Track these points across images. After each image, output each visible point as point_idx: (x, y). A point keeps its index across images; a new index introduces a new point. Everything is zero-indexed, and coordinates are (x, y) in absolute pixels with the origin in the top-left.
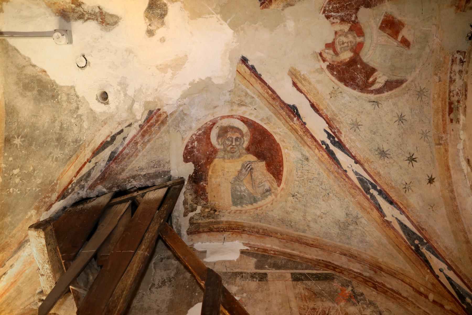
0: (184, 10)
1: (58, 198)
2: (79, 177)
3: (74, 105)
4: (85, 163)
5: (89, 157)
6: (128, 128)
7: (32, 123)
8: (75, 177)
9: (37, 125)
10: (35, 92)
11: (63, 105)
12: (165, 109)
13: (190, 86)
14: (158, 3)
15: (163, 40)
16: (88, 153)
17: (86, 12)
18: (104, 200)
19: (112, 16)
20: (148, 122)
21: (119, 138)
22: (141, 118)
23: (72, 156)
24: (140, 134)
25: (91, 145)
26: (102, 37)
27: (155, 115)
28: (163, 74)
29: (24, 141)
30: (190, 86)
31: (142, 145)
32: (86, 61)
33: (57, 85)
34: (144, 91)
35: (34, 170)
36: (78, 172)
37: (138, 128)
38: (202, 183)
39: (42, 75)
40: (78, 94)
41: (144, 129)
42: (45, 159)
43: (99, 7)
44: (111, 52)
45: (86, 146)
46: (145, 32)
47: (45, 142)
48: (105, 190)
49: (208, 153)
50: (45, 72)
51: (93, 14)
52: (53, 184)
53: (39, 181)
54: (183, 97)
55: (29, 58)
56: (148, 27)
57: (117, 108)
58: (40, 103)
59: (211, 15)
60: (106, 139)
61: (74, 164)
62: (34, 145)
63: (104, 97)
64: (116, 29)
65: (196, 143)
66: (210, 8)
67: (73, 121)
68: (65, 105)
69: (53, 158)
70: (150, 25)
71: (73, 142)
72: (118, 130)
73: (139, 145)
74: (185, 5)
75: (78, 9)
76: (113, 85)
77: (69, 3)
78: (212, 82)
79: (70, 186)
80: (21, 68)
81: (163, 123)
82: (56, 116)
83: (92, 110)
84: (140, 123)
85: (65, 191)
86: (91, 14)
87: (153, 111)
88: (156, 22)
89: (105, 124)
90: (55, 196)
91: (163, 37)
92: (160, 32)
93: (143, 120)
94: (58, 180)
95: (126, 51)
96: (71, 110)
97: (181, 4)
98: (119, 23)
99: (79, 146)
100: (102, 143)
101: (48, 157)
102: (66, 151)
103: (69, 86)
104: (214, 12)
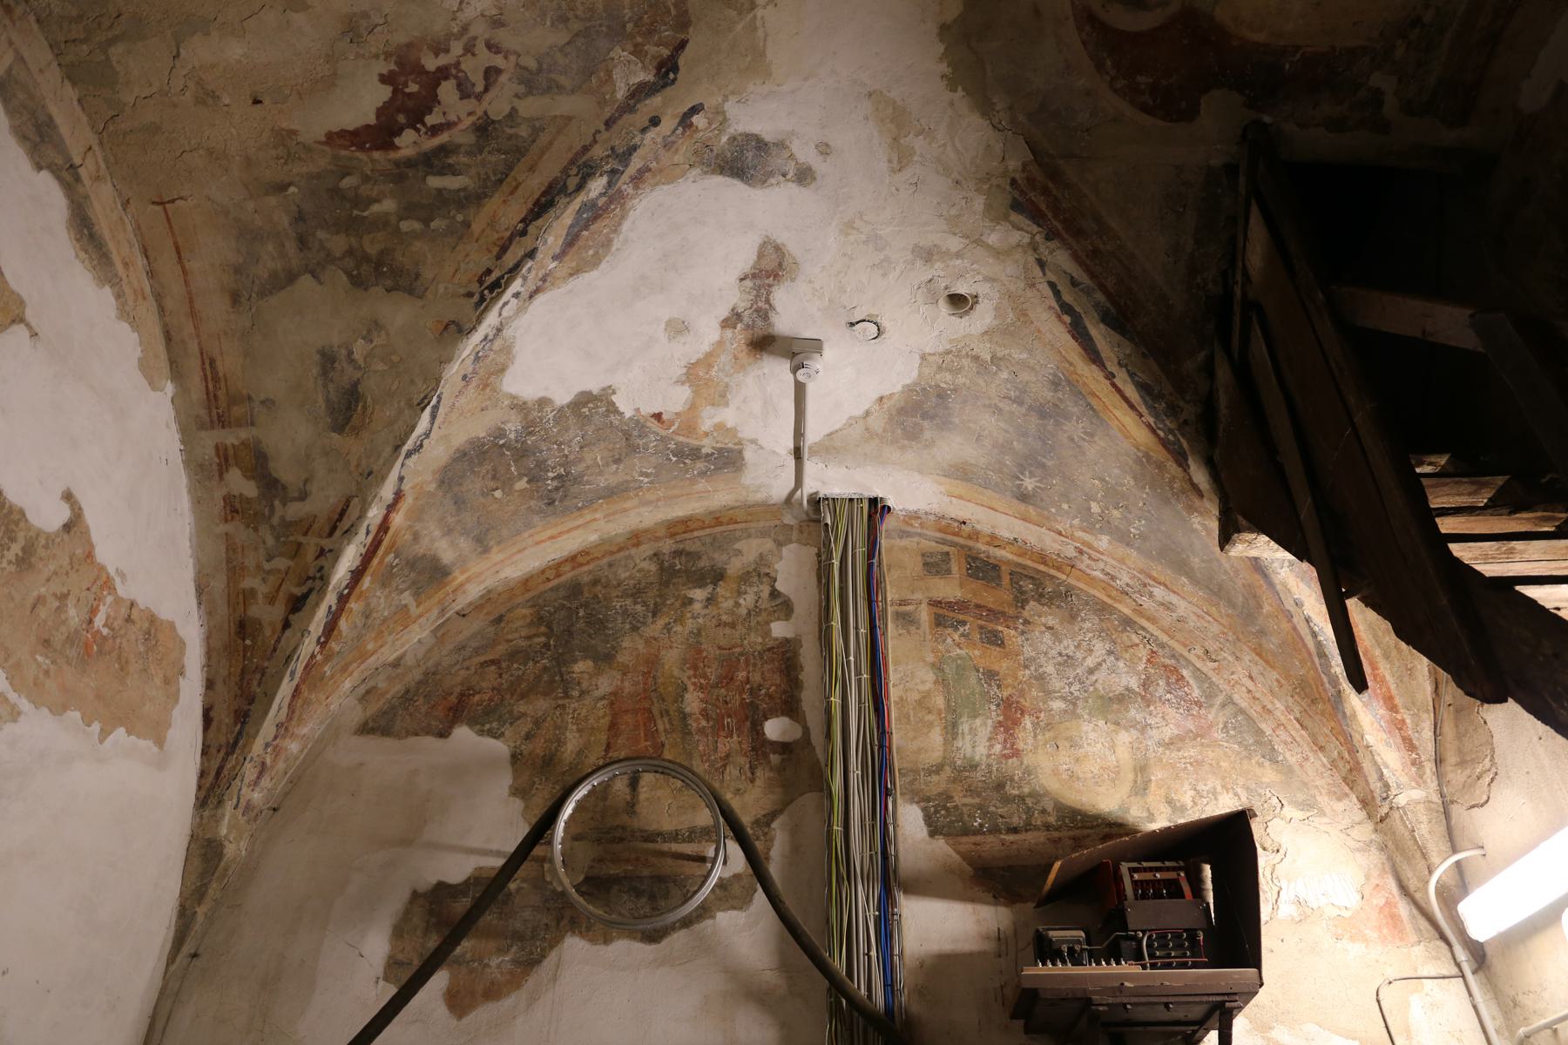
0: (745, 95)
1: (1180, 465)
2: (1143, 409)
3: (966, 362)
4: (1114, 385)
5: (1102, 374)
6: (1047, 271)
7: (993, 447)
8: (1141, 416)
9: (1001, 440)
10: (926, 424)
11: (964, 384)
12: (1013, 164)
13: (960, 88)
14: (729, 155)
15: (824, 149)
16: (1090, 374)
17: (752, 305)
18: (1223, 373)
19: (761, 255)
20: (1043, 216)
21: (1067, 298)
22: (1028, 233)
23: (1089, 404)
24: (1070, 240)
25: (1071, 360)
26: (810, 282)
27: (1026, 194)
28: (916, 158)
29: (1030, 472)
30: (960, 88)
31: (1105, 238)
32: (864, 321)
33: (915, 384)
34: (953, 212)
35: (1102, 480)
36: (1132, 406)
37: (1053, 244)
38: (1287, 66)
39: (887, 404)
40: (941, 349)
41: (1060, 227)
42: (1084, 454)
43: (742, 280)
44: (849, 267)
45: (1072, 368)
46: (803, 189)
47: (1043, 441)
48: (1203, 354)
49: (1185, 42)
50: (881, 399)
51: (758, 292)
52: (1144, 460)
53: (1129, 481)
54: (985, 107)
55: (850, 418)
56: (788, 180)
57: (987, 279)
58: (951, 423)
59: (758, 23)
60: (1065, 323)
61: (1110, 407)
62: (1044, 460)
63: (957, 301)
64: (793, 247)
65: (1141, 79)
66: (739, 27)
67: (1004, 375)
68: (964, 380)
69: (1084, 439)
70: (784, 175)
71: (1056, 391)
72: (1048, 292)
73: (1101, 246)
74: (733, 93)
75: (746, 320)
76: (930, 277)
77: (733, 332)
78: (955, 21)
79: (1161, 434)
80: (870, 434)
81: (1054, 174)
82: (987, 402)
83: (986, 333)
84: (1038, 238)
85: (1171, 447)
86: (756, 296)
87: (1014, 199)
88: (777, 161)
89: (1026, 315)
90: (1172, 466)
91: (817, 146)
92: (805, 153)
93: (1035, 229)
94: (1138, 449)
95: (847, 234)
96: (978, 373)
97: (730, 102)
98: (779, 241)
99: (1069, 382)
100: (1073, 337)
101: (1079, 447)
102: (1075, 410)
103: (921, 364)
104: (751, 15)
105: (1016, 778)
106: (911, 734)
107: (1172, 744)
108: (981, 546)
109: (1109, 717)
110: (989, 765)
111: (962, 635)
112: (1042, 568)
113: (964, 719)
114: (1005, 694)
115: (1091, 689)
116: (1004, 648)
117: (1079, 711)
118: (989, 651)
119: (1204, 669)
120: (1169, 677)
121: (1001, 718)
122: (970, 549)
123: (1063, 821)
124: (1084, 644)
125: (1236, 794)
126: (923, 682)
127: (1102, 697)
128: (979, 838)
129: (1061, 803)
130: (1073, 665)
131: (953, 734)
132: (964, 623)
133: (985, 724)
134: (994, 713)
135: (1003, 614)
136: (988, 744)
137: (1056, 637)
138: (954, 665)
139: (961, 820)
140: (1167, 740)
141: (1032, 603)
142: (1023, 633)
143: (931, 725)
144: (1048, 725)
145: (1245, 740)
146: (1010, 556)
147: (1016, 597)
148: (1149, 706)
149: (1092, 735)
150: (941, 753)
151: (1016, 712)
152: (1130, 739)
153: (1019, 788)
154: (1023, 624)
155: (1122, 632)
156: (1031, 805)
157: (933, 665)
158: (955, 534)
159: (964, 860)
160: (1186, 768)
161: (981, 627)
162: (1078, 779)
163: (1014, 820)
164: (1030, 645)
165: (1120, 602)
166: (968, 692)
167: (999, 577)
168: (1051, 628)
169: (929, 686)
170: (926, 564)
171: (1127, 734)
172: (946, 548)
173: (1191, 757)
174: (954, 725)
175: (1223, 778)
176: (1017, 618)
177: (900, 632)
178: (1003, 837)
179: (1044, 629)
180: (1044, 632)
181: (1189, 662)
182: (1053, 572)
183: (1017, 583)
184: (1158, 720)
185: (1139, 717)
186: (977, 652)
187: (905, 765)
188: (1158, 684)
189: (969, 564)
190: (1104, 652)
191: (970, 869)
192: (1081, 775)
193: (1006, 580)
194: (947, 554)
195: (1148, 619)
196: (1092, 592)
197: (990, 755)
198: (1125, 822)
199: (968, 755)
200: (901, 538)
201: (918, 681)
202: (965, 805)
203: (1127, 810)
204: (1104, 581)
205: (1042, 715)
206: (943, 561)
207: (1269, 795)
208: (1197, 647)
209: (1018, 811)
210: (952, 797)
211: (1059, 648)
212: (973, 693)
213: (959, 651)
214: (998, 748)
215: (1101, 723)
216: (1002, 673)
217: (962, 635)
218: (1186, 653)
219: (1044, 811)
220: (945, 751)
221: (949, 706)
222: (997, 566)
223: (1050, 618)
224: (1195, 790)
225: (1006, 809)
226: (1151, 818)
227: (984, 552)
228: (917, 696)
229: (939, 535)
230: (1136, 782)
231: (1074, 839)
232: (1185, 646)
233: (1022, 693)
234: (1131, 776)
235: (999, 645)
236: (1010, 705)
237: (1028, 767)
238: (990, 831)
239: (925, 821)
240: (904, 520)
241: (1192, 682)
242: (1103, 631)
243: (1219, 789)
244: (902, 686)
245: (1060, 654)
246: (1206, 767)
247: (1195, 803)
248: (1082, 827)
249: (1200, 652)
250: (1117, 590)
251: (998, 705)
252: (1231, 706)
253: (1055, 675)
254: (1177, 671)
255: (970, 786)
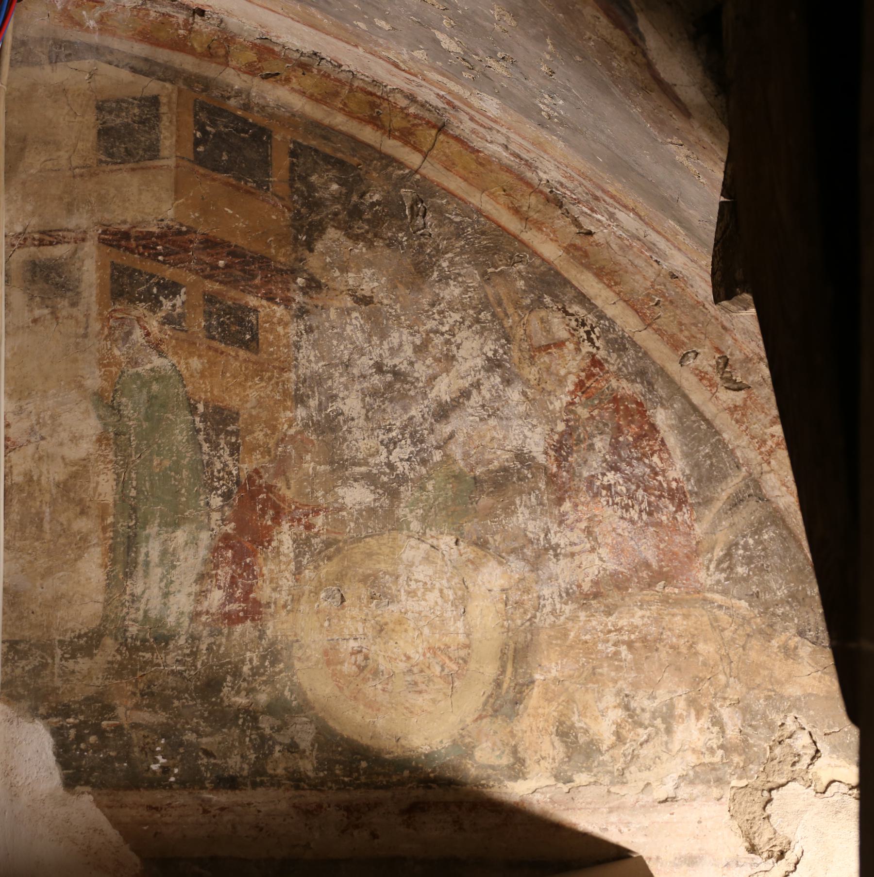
105: (246, 669)
106: (42, 563)
107: (596, 595)
108: (234, 79)
109: (467, 527)
110: (194, 638)
111: (168, 320)
112: (368, 134)
113: (153, 529)
114: (246, 468)
115: (437, 456)
116: (257, 351)
117: (402, 511)
118: (222, 359)
119: (709, 410)
120: (619, 430)
121: (230, 528)
122: (207, 84)
123: (331, 770)
124: (438, 340)
125: (717, 722)
126: (75, 439)
127: (458, 477)
128: (159, 796)
129: (332, 733)
130: (404, 396)
131: (126, 564)
132: (172, 288)
133: (194, 542)
134: (216, 516)
135: (264, 261)
136: (195, 588)
137: (376, 324)
138: (144, 396)
139: (127, 758)
140: (586, 587)
141: (332, 233)
142: (302, 312)
143: (82, 543)
144: (328, 544)
145: (768, 589)
146: (299, 103)
147: (298, 217)
148: (560, 501)
149: (422, 572)
150: (99, 607)
151: (264, 512)
152: (502, 582)
153: (250, 691)
154: (304, 290)
155: (530, 309)
156: (268, 731)
157: (99, 397)
158: (180, 45)
159: (126, 841)
160: (617, 653)
161: (211, 299)
162: (376, 673)
163: (231, 762)
164: (315, 345)
165: (538, 226)
166: (167, 463)
167: (266, 163)
168: (365, 301)
169: (86, 448)
170: (104, 132)
171: (498, 570)
172: (152, 87)
173: (634, 628)
174: (132, 542)
175: (697, 681)
176: (294, 272)
177: (37, 313)
178: (206, 795)
179: (349, 302)
180: (349, 312)
181: (676, 390)
182: (392, 147)
183: (304, 179)
184: (574, 536)
185: (533, 528)
186: (196, 363)
187: (27, 634)
188: (591, 447)
189: (201, 127)
190: (480, 362)
191: (136, 859)
192: (383, 665)
193: (281, 164)
194: (154, 101)
195: (600, 273)
196: (477, 199)
197: (198, 614)
198: (460, 776)
199: (153, 614)
200: (54, 60)
201: (64, 436)
202: (135, 726)
203: (468, 751)
204: (508, 170)
205: (319, 520)
206: (142, 122)
207: (791, 726)
208: (705, 350)
209: (242, 743)
210: (111, 709)
211: (380, 351)
212: (177, 468)
213: (157, 361)
214: (217, 596)
215: (446, 541)
216: (244, 415)
217: (168, 320)
218: (673, 367)
219: (292, 748)
220: (107, 602)
221: (123, 497)
222: (263, 130)
223: (368, 272)
224: (627, 708)
225: (218, 738)
226: (518, 770)
227: (239, 93)
228: (56, 473)
229: (141, 49)
230: (498, 684)
231: (348, 809)
232: (675, 344)
233: (282, 466)
234: (490, 670)
235: (246, 345)
236: (253, 496)
237: (273, 644)
238: (183, 783)
239: (57, 755)
240: (65, 9)
241: (672, 440)
242: (485, 305)
243: (681, 706)
244: (31, 449)
245: (379, 368)
246: (664, 654)
247: (620, 738)
248: (367, 785)
249: (706, 361)
250: (536, 191)
251: (227, 496)
252: (753, 503)
253: (361, 422)
254: (643, 414)
255: (150, 683)
